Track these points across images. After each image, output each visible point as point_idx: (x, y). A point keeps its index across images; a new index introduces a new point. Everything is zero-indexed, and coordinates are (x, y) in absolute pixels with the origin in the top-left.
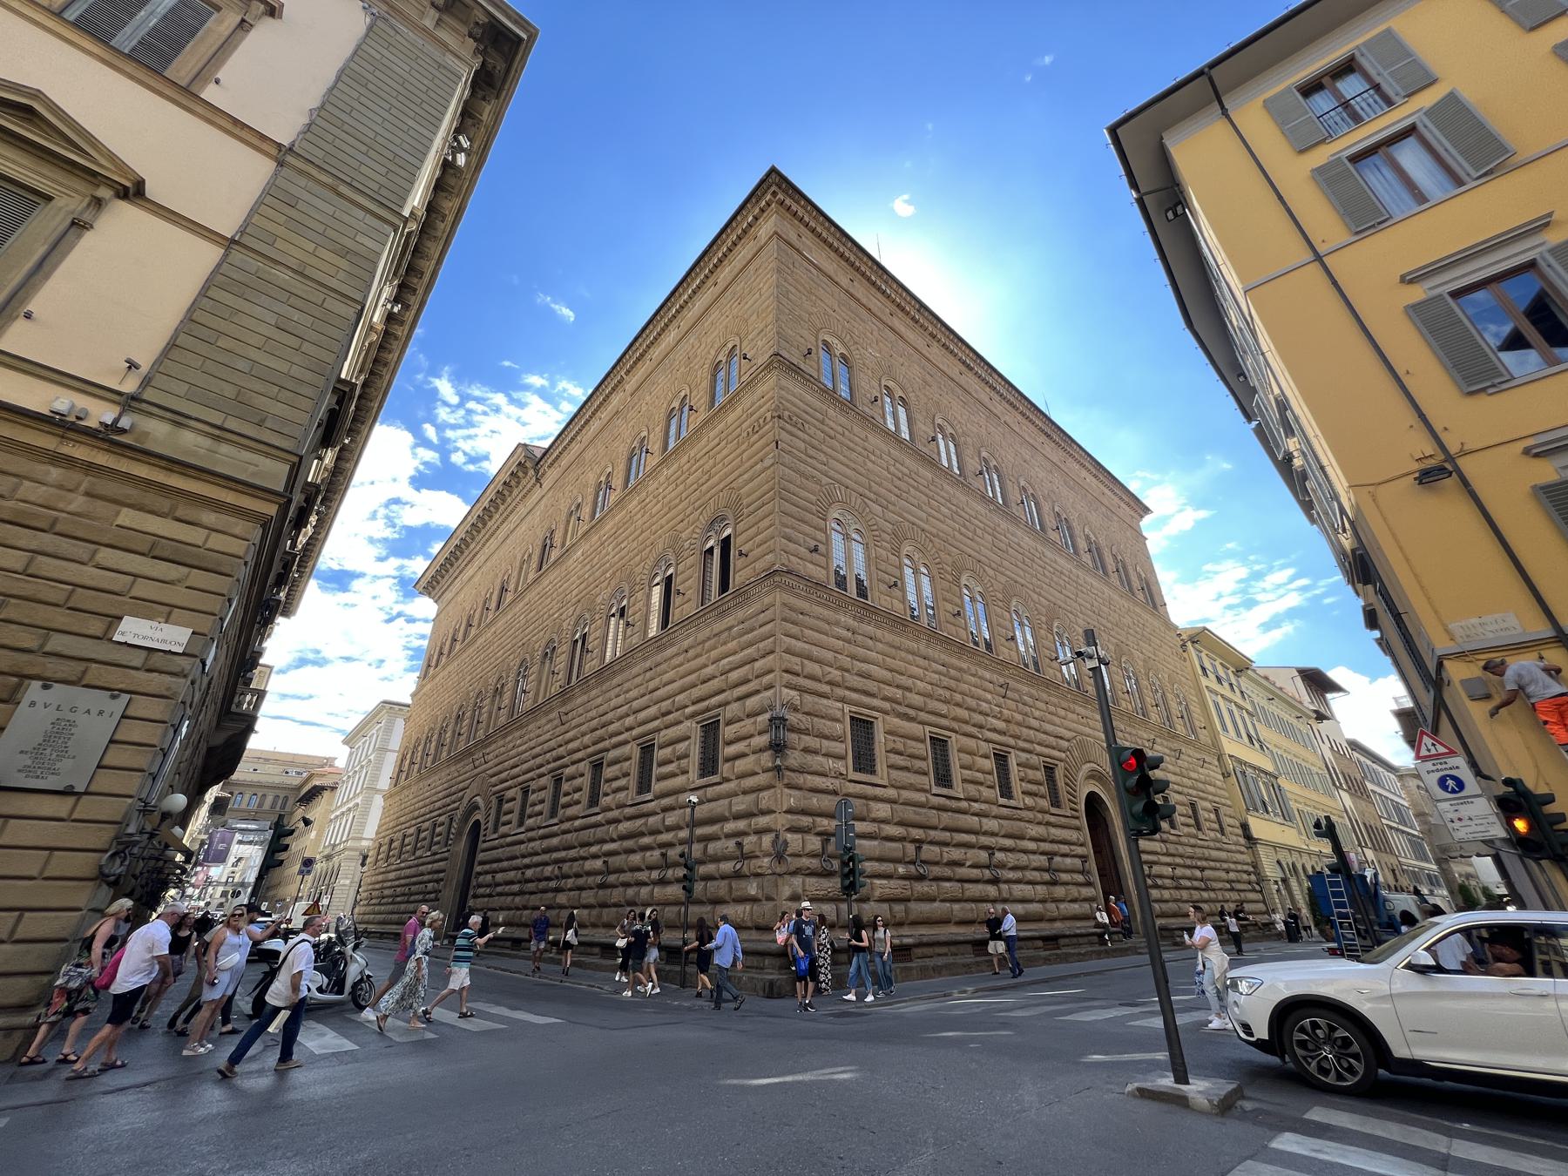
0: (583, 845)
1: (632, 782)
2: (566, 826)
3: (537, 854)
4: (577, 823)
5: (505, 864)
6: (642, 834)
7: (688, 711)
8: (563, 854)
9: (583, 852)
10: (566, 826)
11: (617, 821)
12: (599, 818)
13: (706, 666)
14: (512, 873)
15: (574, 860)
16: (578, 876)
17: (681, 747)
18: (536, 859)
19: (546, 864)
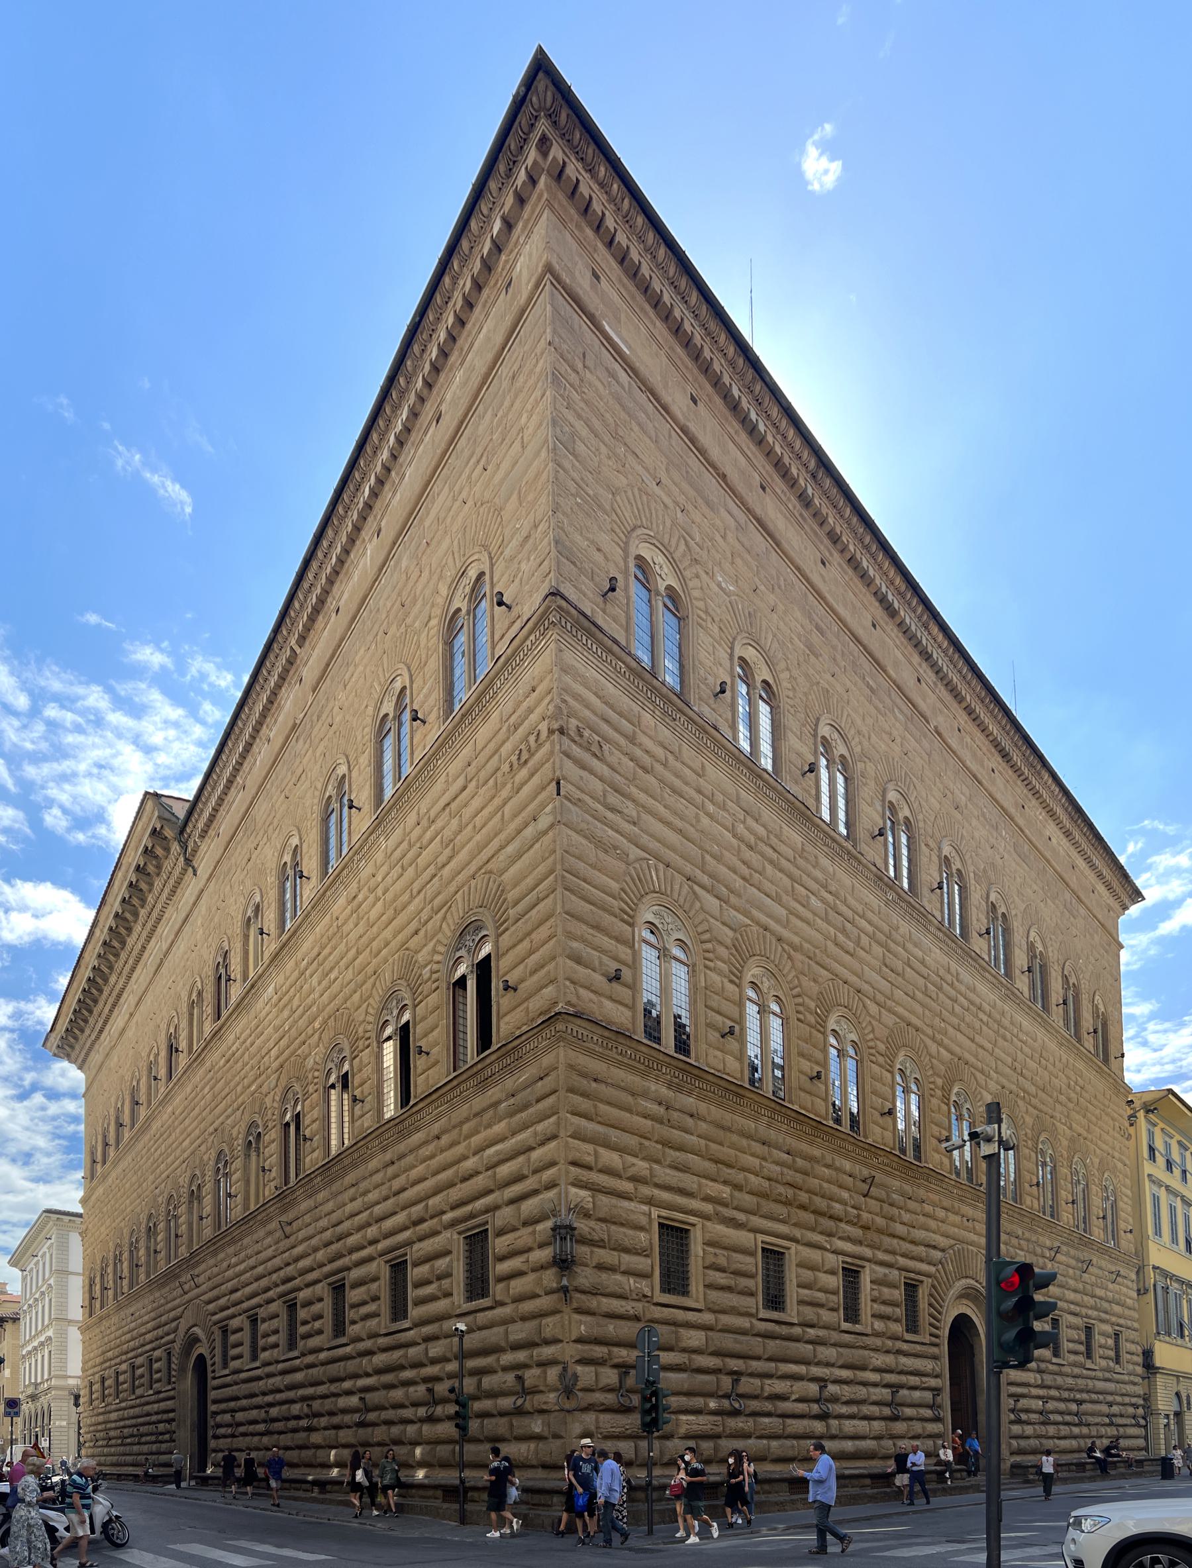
0: (333, 1380)
1: (384, 1305)
2: (310, 1359)
3: (280, 1391)
4: (323, 1356)
5: (244, 1402)
6: (402, 1368)
7: (447, 1217)
8: (310, 1391)
9: (334, 1388)
10: (310, 1359)
11: (370, 1353)
12: (348, 1349)
13: (465, 1158)
14: (254, 1414)
15: (324, 1397)
16: (331, 1414)
17: (441, 1264)
18: (279, 1397)
19: (293, 1402)
